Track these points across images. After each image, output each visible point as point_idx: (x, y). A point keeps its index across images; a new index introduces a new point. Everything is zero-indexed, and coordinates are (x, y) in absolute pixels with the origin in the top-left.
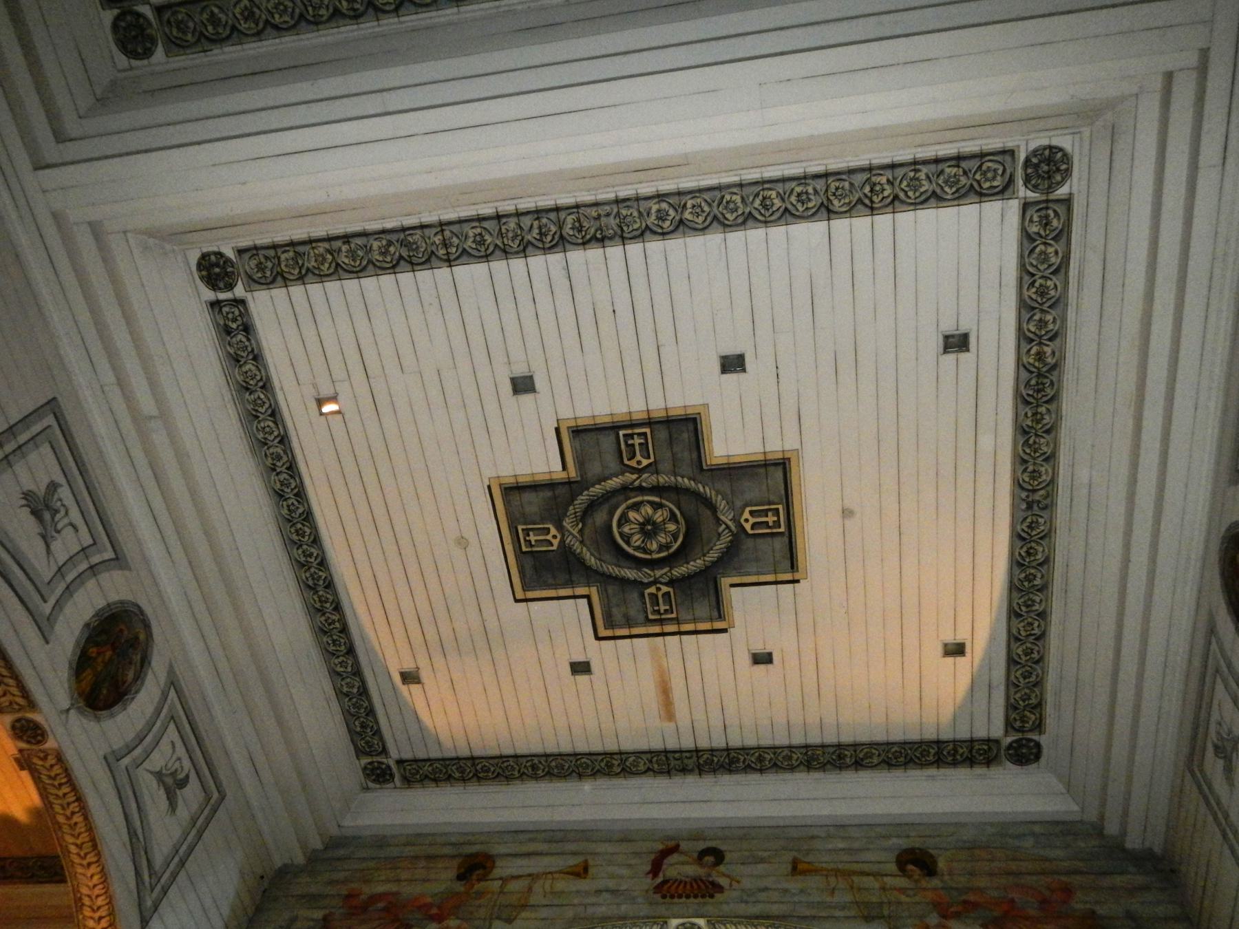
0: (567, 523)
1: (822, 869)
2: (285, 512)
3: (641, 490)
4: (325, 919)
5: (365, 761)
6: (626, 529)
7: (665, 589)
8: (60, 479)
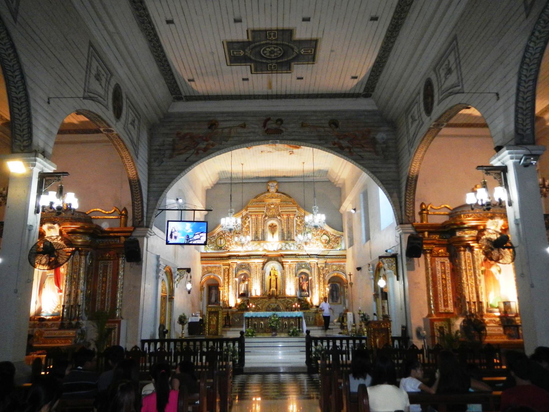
0: (247, 50)
1: (310, 125)
2: (152, 45)
3: (272, 44)
4: (173, 141)
5: (174, 96)
6: (265, 52)
7: (274, 64)
8: (98, 64)
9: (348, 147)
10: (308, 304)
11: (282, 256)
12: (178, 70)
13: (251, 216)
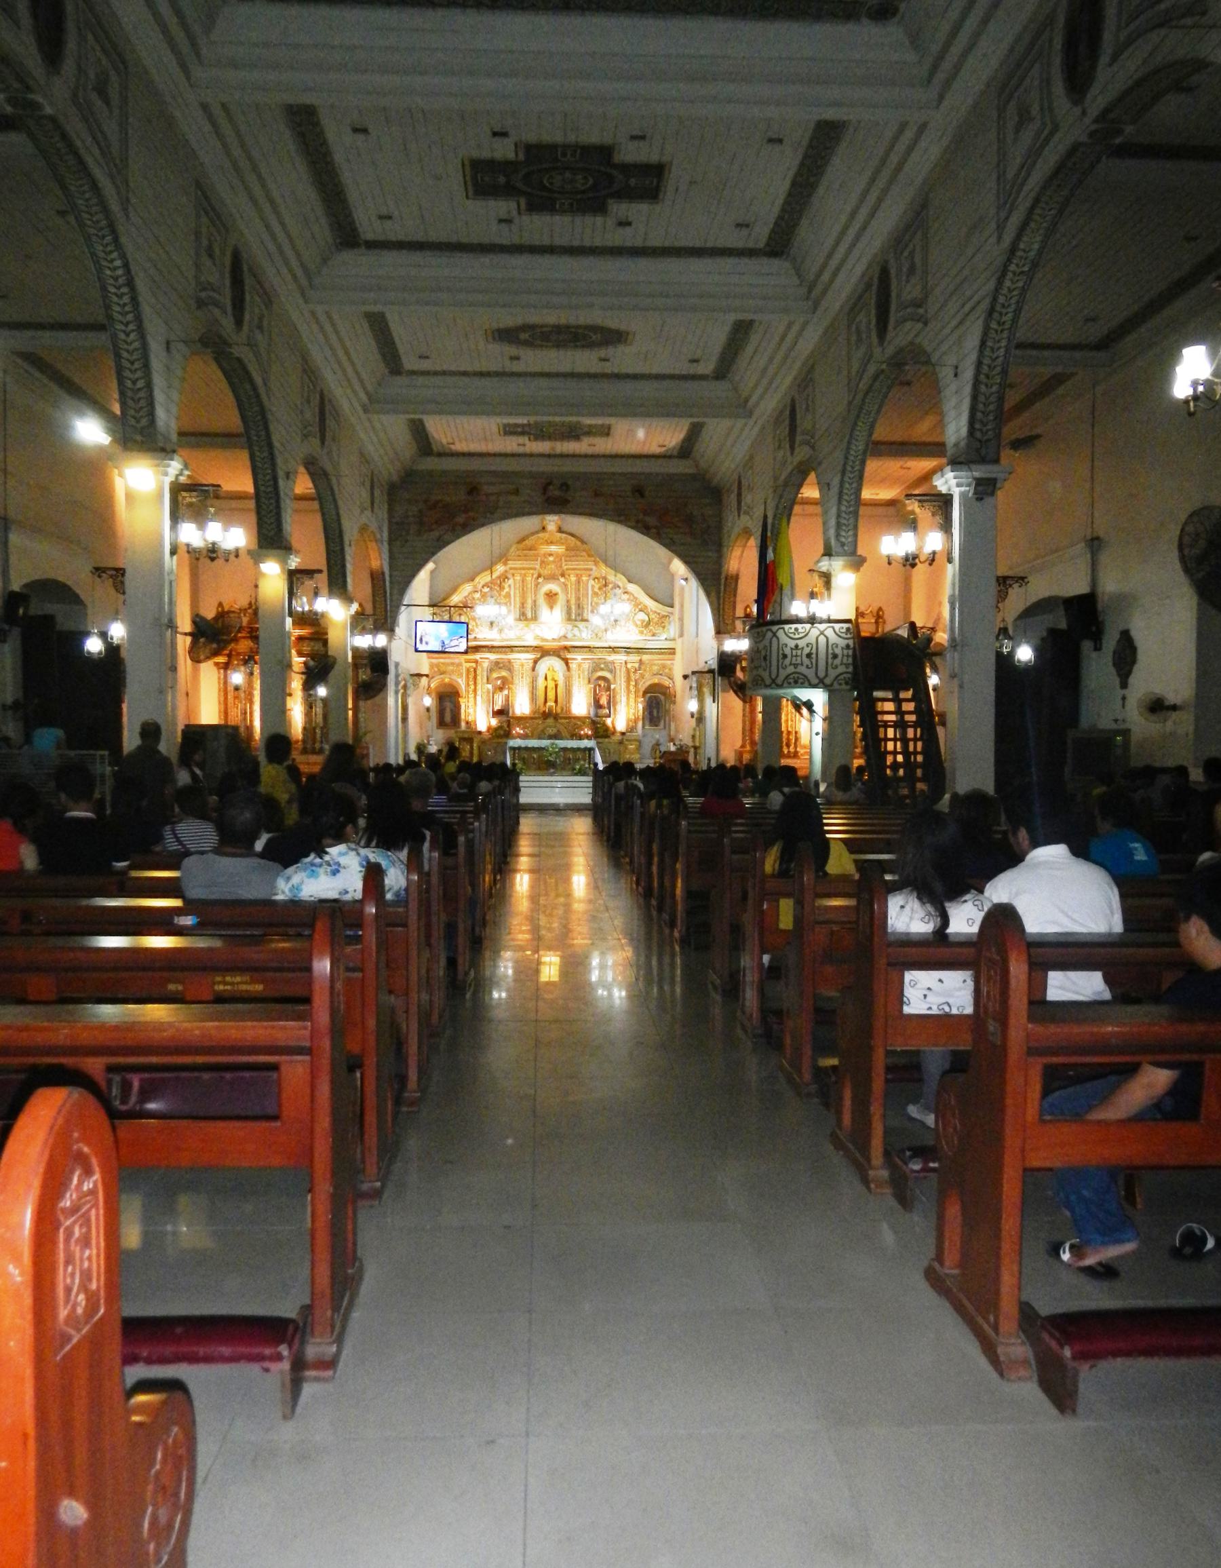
4: (420, 511)
9: (656, 527)
10: (606, 729)
11: (566, 648)
12: (436, 436)
13: (513, 575)
